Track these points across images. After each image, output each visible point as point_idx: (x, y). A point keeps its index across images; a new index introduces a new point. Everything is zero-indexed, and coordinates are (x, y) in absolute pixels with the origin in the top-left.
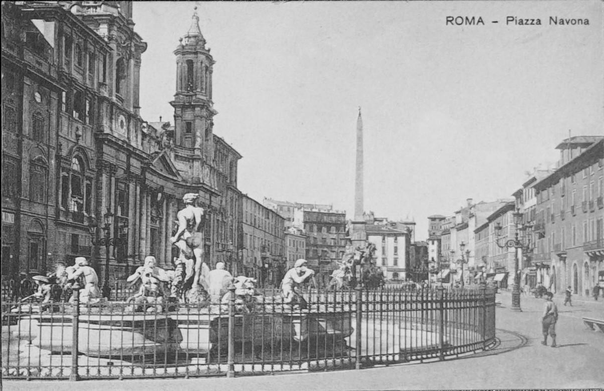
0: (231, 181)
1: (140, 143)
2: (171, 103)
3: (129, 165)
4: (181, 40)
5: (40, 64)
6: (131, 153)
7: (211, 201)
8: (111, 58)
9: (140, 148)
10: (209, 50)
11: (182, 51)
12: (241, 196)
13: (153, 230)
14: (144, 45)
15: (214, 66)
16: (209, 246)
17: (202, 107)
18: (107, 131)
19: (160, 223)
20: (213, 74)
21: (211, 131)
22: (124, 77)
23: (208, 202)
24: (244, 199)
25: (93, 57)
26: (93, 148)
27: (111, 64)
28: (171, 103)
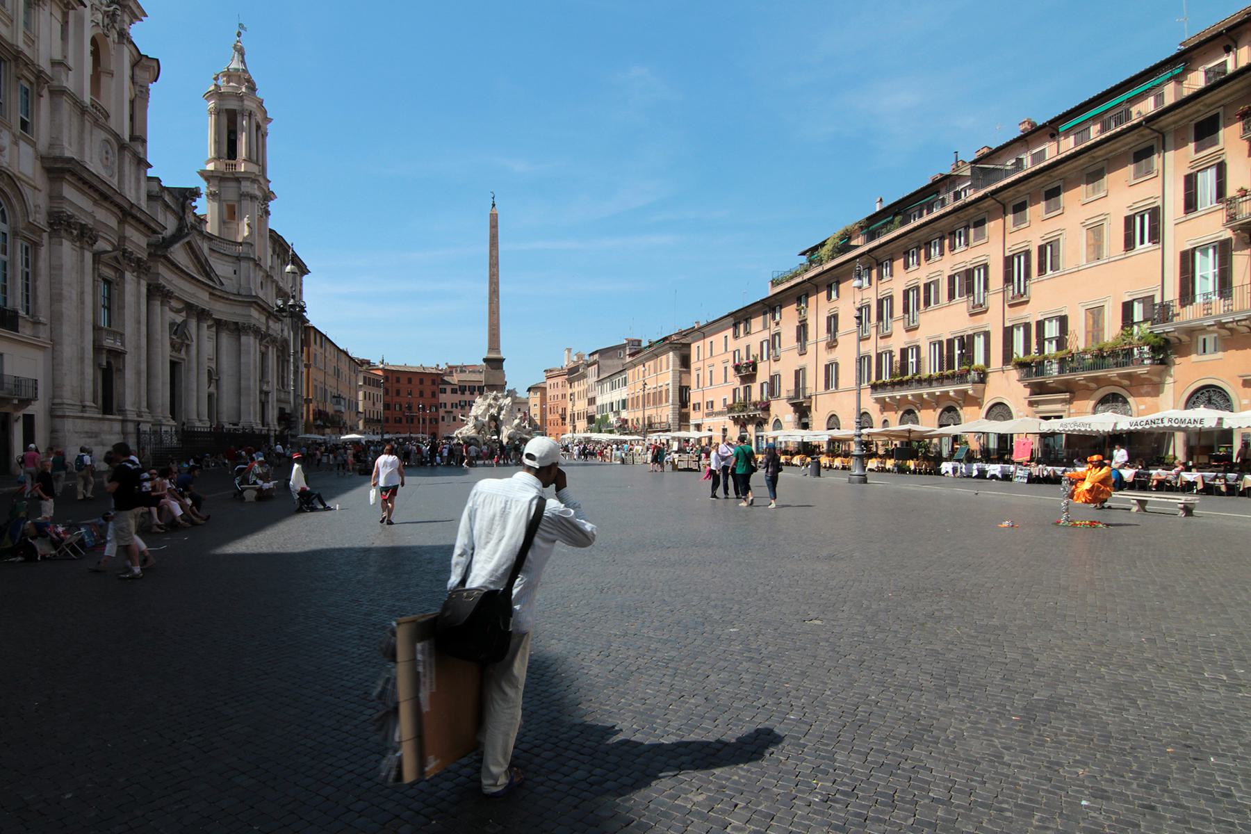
3: (123, 238)
6: (127, 213)
7: (268, 327)
11: (217, 94)
13: (174, 365)
14: (155, 64)
15: (269, 126)
16: (267, 393)
17: (254, 181)
20: (269, 140)
21: (266, 224)
23: (264, 329)
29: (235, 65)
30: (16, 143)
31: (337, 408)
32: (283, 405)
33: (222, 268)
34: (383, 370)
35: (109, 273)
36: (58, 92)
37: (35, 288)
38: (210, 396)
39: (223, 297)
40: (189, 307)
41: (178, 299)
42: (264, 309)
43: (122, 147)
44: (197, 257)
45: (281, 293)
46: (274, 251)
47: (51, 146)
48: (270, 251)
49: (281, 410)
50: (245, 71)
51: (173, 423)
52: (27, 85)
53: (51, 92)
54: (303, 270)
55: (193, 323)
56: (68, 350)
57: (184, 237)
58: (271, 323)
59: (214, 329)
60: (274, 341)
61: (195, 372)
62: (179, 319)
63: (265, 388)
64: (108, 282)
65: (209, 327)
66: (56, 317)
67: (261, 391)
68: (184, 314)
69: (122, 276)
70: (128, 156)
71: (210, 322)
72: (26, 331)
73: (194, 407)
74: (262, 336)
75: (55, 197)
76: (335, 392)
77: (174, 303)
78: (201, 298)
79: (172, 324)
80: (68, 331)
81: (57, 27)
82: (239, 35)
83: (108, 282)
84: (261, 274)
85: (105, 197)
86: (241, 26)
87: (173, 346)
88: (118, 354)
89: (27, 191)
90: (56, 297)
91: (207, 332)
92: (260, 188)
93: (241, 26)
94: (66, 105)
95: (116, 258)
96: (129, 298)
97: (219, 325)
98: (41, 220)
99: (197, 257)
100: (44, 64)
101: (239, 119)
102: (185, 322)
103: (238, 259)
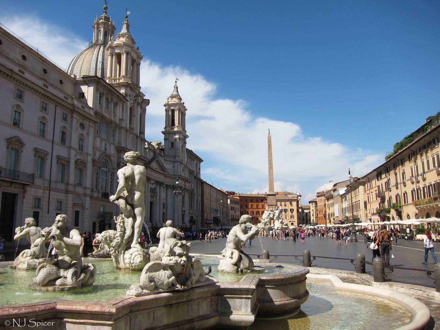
0: (196, 174)
1: (143, 153)
2: (163, 132)
4: (168, 99)
5: (84, 108)
7: (185, 186)
8: (127, 106)
9: (144, 155)
10: (184, 103)
12: (203, 183)
15: (186, 112)
16: (184, 211)
18: (123, 145)
19: (156, 198)
21: (185, 146)
22: (135, 116)
23: (183, 186)
24: (205, 185)
25: (116, 105)
26: (116, 154)
27: (127, 109)
28: (163, 132)
29: (175, 93)
30: (110, 146)
31: (216, 215)
32: (192, 215)
33: (168, 166)
34: (239, 197)
36: (121, 128)
37: (113, 185)
38: (163, 213)
39: (169, 176)
40: (157, 182)
41: (153, 180)
42: (183, 179)
43: (137, 137)
44: (159, 164)
45: (191, 172)
46: (188, 156)
47: (119, 143)
48: (186, 157)
49: (192, 218)
50: (178, 95)
51: (151, 224)
52: (113, 128)
53: (119, 128)
54: (200, 160)
55: (158, 187)
57: (155, 159)
58: (187, 184)
59: (165, 188)
60: (188, 190)
61: (158, 205)
62: (153, 187)
63: (184, 209)
65: (164, 188)
67: (182, 211)
68: (155, 185)
70: (139, 139)
71: (164, 186)
73: (158, 218)
74: (184, 189)
76: (215, 208)
77: (152, 181)
78: (161, 178)
79: (151, 189)
81: (121, 109)
82: (176, 82)
84: (182, 166)
86: (177, 79)
87: (151, 196)
89: (112, 158)
91: (163, 190)
92: (183, 135)
93: (177, 79)
94: (123, 130)
97: (167, 186)
99: (159, 164)
100: (118, 121)
101: (175, 112)
102: (155, 188)
103: (174, 162)
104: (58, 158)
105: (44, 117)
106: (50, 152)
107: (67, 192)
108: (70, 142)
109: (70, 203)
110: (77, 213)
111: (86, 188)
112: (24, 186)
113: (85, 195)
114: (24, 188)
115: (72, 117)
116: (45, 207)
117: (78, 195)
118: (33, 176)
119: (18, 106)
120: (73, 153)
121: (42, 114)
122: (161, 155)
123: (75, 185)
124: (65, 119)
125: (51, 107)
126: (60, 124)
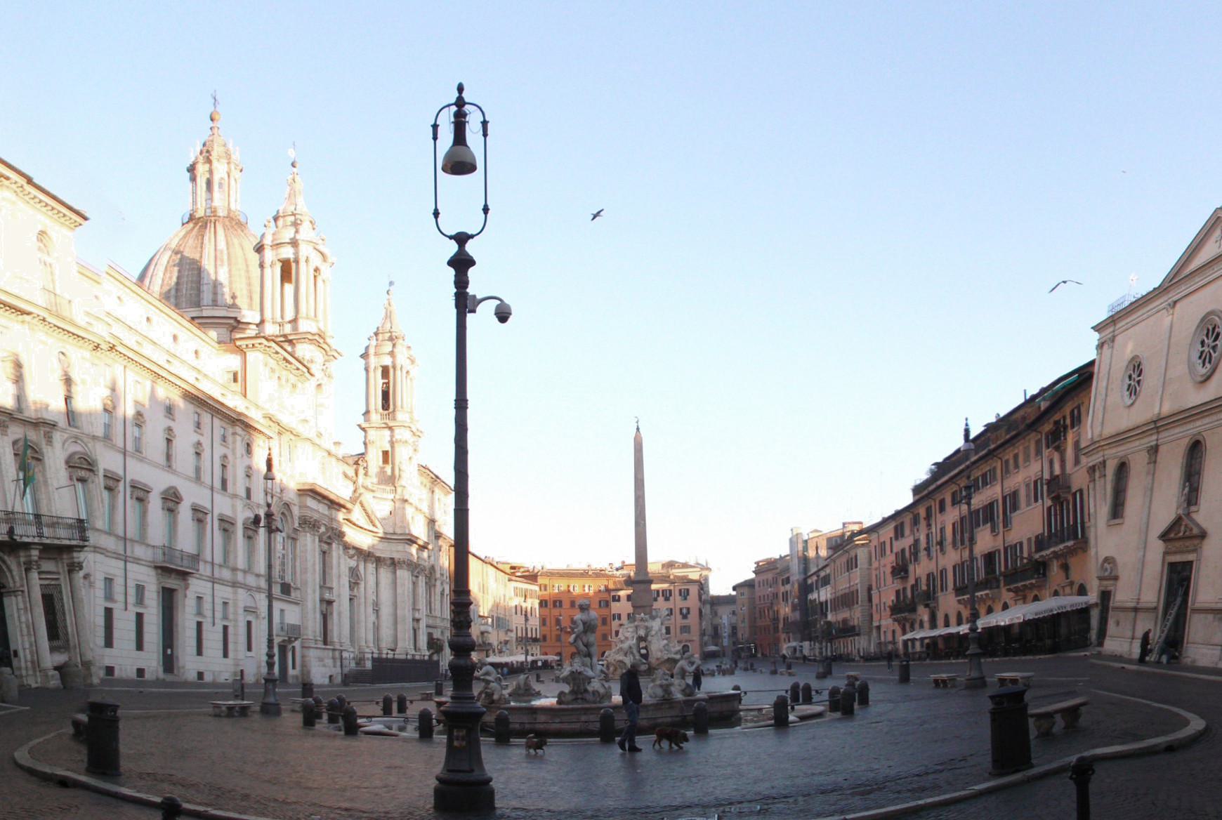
35: (325, 547)
56: (310, 605)
64: (324, 553)
66: (305, 583)
69: (329, 544)
72: (293, 594)
75: (303, 506)
77: (352, 552)
80: (310, 591)
83: (324, 553)
85: (324, 497)
88: (330, 603)
90: (304, 571)
95: (329, 537)
96: (335, 561)
98: (296, 525)
104: (222, 520)
105: (199, 443)
106: (209, 507)
107: (234, 585)
108: (234, 484)
109: (241, 605)
110: (249, 623)
111: (258, 576)
112: (184, 575)
113: (259, 589)
114: (185, 580)
115: (234, 434)
116: (208, 613)
117: (248, 588)
118: (196, 558)
119: (170, 429)
120: (239, 505)
121: (195, 438)
122: (366, 488)
123: (245, 572)
124: (224, 439)
125: (206, 418)
126: (219, 450)
